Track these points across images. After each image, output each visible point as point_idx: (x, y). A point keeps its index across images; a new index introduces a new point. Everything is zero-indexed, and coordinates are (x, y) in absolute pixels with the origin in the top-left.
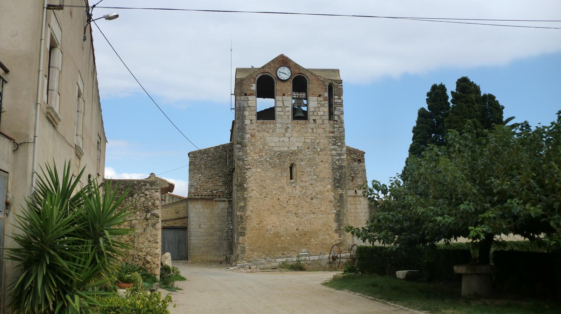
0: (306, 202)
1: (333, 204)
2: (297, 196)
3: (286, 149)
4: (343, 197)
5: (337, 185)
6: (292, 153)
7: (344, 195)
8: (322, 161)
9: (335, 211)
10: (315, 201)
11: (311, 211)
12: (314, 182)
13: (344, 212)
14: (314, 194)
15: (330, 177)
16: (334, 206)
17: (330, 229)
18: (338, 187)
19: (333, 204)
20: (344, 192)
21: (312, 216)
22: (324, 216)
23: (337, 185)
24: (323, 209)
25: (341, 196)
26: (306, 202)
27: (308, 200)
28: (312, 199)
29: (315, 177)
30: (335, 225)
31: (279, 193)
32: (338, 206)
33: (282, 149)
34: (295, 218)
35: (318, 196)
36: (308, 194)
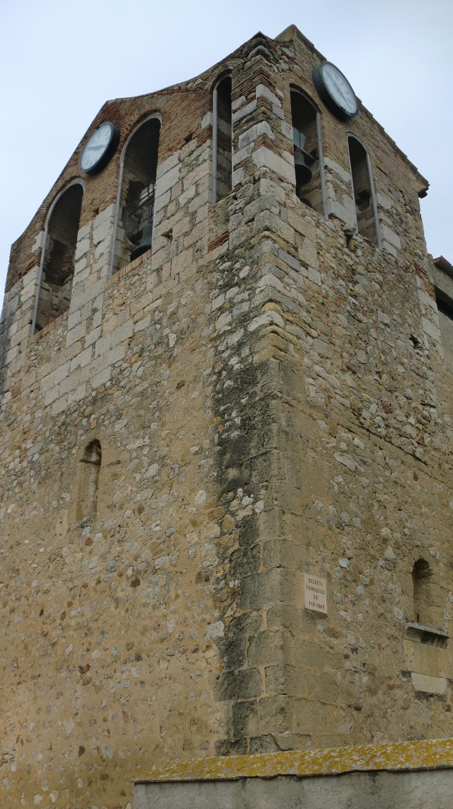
0: (117, 601)
1: (210, 587)
2: (92, 584)
3: (81, 394)
4: (255, 533)
5: (232, 473)
6: (94, 401)
7: (261, 523)
8: (180, 386)
9: (218, 630)
10: (146, 590)
11: (129, 646)
12: (148, 493)
13: (258, 622)
14: (146, 554)
15: (206, 443)
16: (218, 601)
17: (197, 739)
18: (233, 486)
19: (210, 587)
20: (260, 505)
21: (135, 671)
22: (179, 662)
23: (232, 473)
24: (171, 626)
25: (247, 528)
26: (117, 601)
27: (124, 590)
28: (135, 583)
29: (154, 469)
30: (217, 714)
31: (47, 585)
32: (234, 594)
33: (72, 398)
34: (79, 687)
35: (159, 562)
36: (127, 559)
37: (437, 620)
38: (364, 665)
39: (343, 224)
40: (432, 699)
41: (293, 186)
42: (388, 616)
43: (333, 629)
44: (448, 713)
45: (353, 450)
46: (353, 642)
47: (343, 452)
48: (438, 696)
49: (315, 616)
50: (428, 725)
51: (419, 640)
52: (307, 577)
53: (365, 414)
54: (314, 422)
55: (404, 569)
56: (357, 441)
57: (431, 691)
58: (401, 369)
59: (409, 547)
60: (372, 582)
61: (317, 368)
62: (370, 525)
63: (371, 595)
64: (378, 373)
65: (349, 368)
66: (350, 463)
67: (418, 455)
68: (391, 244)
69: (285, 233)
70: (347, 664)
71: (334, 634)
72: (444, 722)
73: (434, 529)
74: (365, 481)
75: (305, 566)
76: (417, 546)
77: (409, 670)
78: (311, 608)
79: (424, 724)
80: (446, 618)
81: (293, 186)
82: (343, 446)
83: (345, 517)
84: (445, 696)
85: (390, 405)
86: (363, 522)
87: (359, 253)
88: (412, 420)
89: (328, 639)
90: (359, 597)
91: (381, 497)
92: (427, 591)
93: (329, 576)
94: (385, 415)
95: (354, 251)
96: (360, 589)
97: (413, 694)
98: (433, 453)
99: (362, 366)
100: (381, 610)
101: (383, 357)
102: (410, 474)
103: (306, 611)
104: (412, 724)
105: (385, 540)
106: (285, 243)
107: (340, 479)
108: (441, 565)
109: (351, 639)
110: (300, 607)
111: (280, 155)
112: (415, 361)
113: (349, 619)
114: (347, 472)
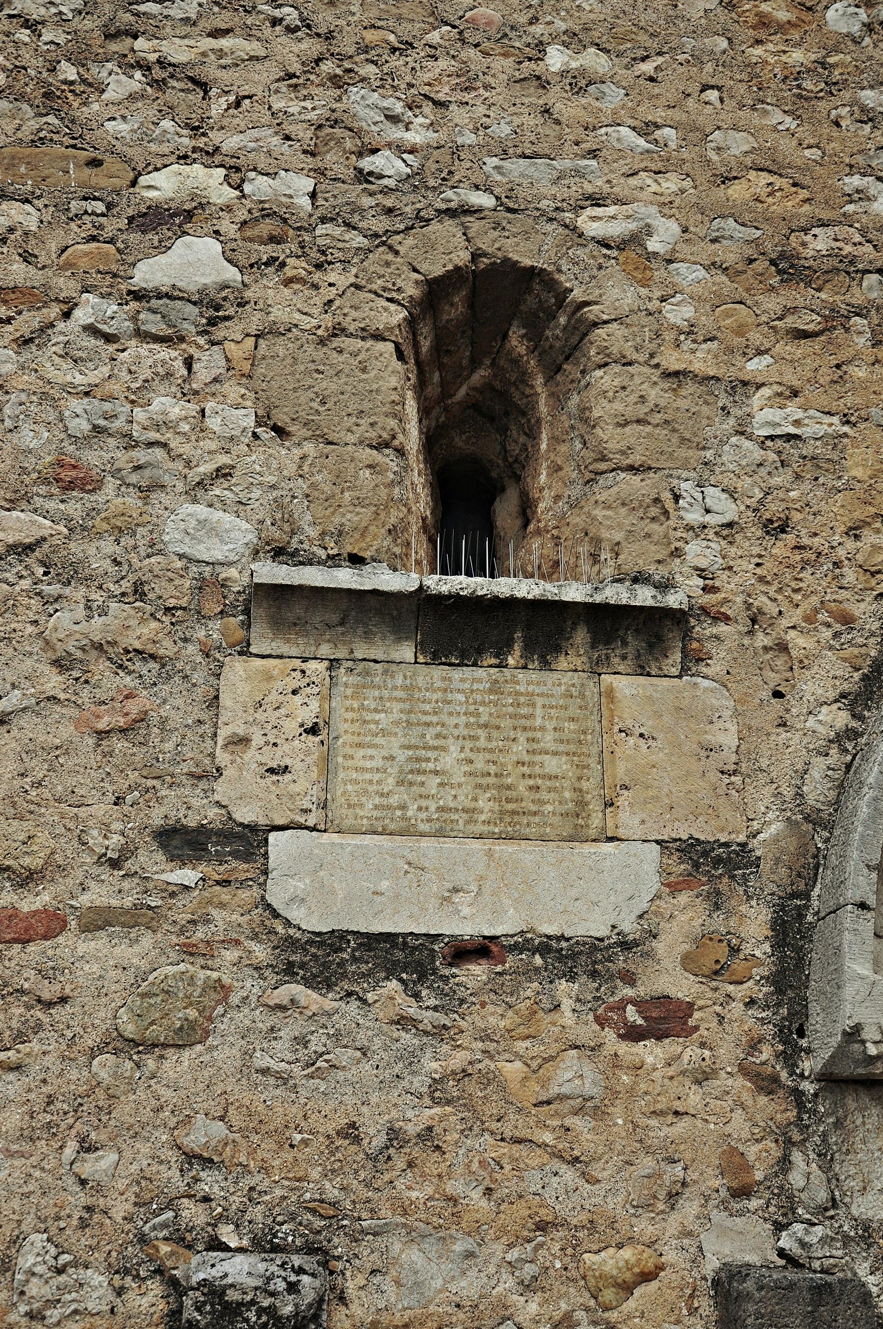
37: (618, 536)
40: (476, 973)
42: (98, 554)
44: (651, 1052)
48: (544, 949)
50: (394, 1135)
51: (406, 652)
55: (308, 323)
57: (467, 925)
59: (380, 224)
72: (586, 1106)
73: (646, 129)
77: (245, 814)
79: (351, 1132)
80: (694, 517)
84: (626, 945)
92: (584, 415)
97: (261, 952)
104: (203, 1134)
108: (689, 275)
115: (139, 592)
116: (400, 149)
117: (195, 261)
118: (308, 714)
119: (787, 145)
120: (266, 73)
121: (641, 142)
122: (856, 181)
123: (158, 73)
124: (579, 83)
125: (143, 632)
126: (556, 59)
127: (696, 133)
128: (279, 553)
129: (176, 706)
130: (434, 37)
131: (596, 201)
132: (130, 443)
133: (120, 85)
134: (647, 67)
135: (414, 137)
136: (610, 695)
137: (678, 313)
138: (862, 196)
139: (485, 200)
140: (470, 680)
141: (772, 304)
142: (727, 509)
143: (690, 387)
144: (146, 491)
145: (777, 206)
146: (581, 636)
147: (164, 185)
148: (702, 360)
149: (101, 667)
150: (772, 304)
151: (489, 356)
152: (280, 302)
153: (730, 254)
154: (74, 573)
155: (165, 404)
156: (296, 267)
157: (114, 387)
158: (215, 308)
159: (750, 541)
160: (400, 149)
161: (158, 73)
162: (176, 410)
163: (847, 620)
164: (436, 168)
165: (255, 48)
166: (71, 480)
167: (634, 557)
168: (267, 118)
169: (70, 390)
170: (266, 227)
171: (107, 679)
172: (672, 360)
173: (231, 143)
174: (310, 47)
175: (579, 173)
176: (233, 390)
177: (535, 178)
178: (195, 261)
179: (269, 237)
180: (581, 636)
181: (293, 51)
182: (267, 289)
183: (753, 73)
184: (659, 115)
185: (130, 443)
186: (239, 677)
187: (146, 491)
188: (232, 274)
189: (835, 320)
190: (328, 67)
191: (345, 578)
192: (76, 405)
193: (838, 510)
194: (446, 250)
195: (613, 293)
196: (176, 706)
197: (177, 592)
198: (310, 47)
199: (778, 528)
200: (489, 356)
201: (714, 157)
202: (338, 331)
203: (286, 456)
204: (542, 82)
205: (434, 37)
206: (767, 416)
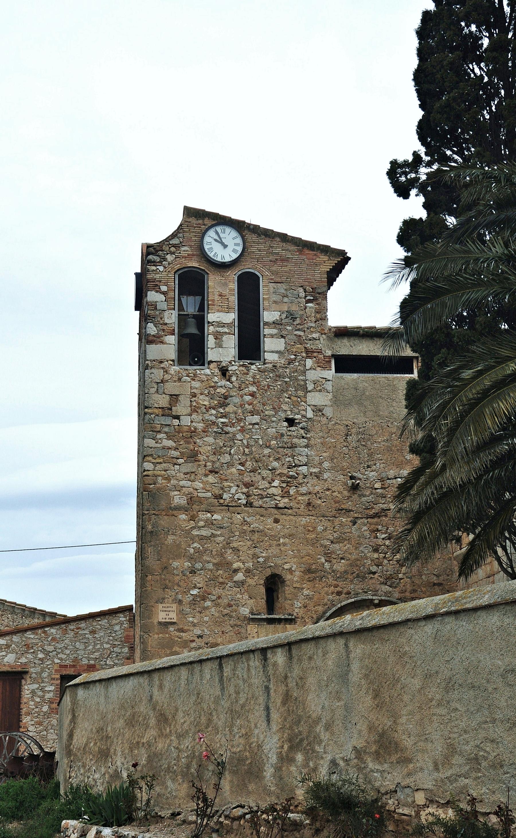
38: (207, 644)
39: (219, 363)
41: (173, 361)
42: (234, 614)
43: (182, 628)
45: (209, 523)
46: (199, 632)
47: (199, 528)
49: (166, 624)
52: (160, 606)
53: (225, 496)
54: (176, 518)
56: (216, 516)
58: (267, 451)
59: (260, 570)
60: (219, 597)
61: (182, 483)
62: (223, 564)
63: (217, 605)
64: (240, 464)
65: (211, 472)
66: (204, 532)
67: (280, 505)
68: (273, 352)
69: (161, 403)
70: (193, 645)
71: (182, 630)
74: (221, 539)
75: (162, 600)
76: (271, 566)
78: (163, 620)
80: (296, 606)
81: (173, 361)
82: (202, 523)
83: (198, 566)
85: (252, 481)
86: (214, 564)
87: (234, 379)
88: (276, 483)
89: (178, 634)
90: (207, 608)
91: (235, 545)
93: (180, 602)
94: (245, 490)
95: (229, 380)
96: (208, 603)
98: (300, 498)
99: (225, 465)
100: (226, 611)
101: (247, 450)
102: (270, 520)
103: (160, 623)
105: (236, 571)
106: (160, 410)
107: (195, 545)
108: (297, 573)
109: (198, 631)
110: (155, 622)
111: (162, 342)
112: (285, 439)
113: (195, 621)
114: (202, 538)
115: (238, 619)
116: (262, 557)
117: (240, 576)
118: (256, 631)
119: (311, 551)
120: (246, 548)
121: (292, 553)
122: (319, 557)
123: (233, 549)
124: (285, 544)
125: (239, 623)
126: (282, 540)
127: (299, 551)
128: (253, 614)
129: (243, 631)
130: (266, 539)
131: (286, 563)
132: (235, 601)
133: (229, 551)
134: (293, 541)
135: (264, 555)
136: (286, 627)
137: (295, 579)
138: (320, 559)
139: (272, 564)
140: (272, 626)
141: (307, 577)
142: (300, 605)
143: (297, 589)
144: (238, 607)
145: (309, 562)
146: (283, 621)
147: (235, 566)
148: (298, 585)
149: (236, 627)
150: (307, 577)
151: (273, 585)
152: (250, 581)
153: (302, 570)
154: (231, 617)
155: (239, 596)
156: (252, 576)
157: (233, 594)
158: (243, 583)
159: (302, 609)
160: (262, 557)
161: (233, 549)
162: (240, 596)
163: (312, 617)
164: (267, 559)
165: (244, 544)
166: (230, 605)
167: (290, 611)
168: (246, 555)
169: (229, 595)
170: (247, 571)
171: (237, 628)
172: (295, 586)
173: (242, 558)
174: (251, 543)
175: (284, 559)
176: (246, 594)
177: (279, 562)
178: (240, 576)
179: (248, 571)
180: (283, 621)
181: (249, 543)
182: (248, 580)
183: (307, 540)
184: (294, 549)
185: (235, 601)
186: (249, 627)
187: (238, 607)
188: (244, 578)
189: (315, 578)
190: (253, 545)
191: (259, 617)
192: (229, 596)
193: (312, 604)
194: (268, 572)
195: (288, 577)
196: (243, 631)
197: (242, 618)
198: (251, 543)
199: (305, 607)
200: (273, 585)
201: (301, 554)
202: (257, 584)
203: (252, 601)
204: (279, 545)
205: (266, 539)
206: (306, 592)
